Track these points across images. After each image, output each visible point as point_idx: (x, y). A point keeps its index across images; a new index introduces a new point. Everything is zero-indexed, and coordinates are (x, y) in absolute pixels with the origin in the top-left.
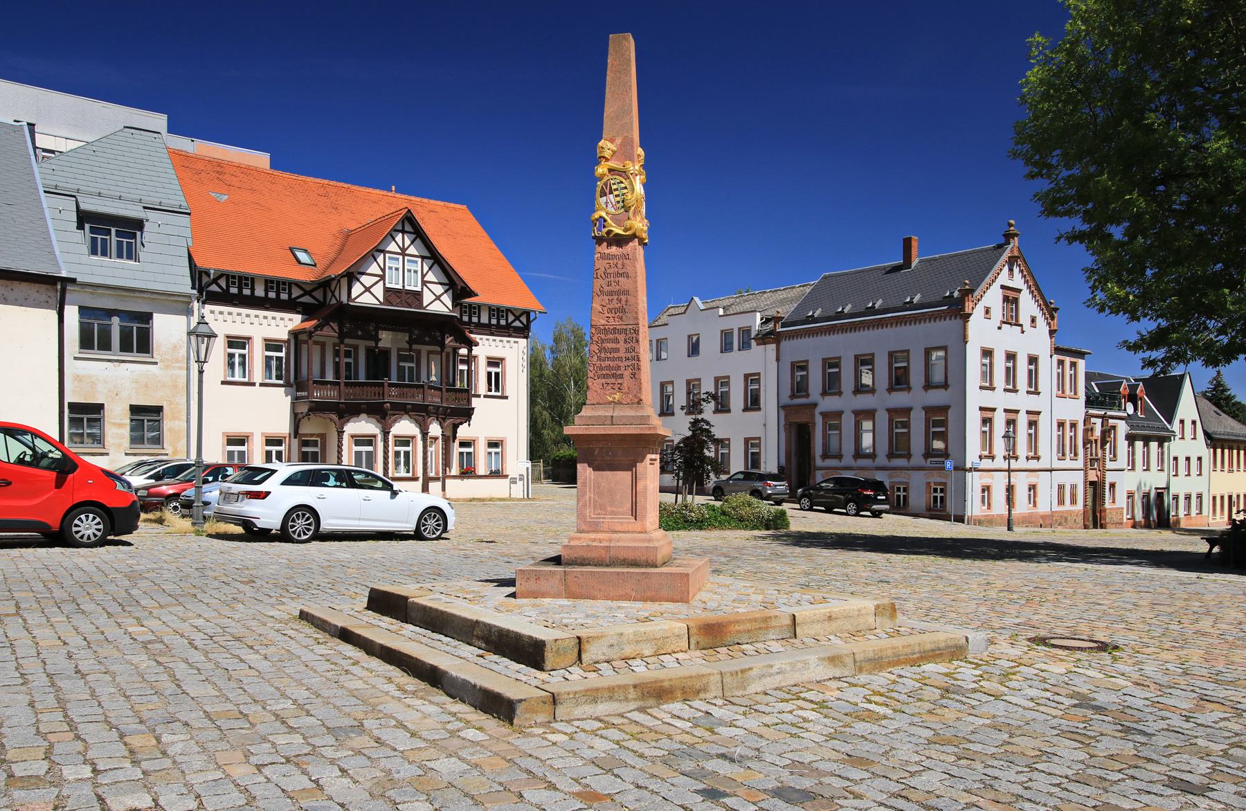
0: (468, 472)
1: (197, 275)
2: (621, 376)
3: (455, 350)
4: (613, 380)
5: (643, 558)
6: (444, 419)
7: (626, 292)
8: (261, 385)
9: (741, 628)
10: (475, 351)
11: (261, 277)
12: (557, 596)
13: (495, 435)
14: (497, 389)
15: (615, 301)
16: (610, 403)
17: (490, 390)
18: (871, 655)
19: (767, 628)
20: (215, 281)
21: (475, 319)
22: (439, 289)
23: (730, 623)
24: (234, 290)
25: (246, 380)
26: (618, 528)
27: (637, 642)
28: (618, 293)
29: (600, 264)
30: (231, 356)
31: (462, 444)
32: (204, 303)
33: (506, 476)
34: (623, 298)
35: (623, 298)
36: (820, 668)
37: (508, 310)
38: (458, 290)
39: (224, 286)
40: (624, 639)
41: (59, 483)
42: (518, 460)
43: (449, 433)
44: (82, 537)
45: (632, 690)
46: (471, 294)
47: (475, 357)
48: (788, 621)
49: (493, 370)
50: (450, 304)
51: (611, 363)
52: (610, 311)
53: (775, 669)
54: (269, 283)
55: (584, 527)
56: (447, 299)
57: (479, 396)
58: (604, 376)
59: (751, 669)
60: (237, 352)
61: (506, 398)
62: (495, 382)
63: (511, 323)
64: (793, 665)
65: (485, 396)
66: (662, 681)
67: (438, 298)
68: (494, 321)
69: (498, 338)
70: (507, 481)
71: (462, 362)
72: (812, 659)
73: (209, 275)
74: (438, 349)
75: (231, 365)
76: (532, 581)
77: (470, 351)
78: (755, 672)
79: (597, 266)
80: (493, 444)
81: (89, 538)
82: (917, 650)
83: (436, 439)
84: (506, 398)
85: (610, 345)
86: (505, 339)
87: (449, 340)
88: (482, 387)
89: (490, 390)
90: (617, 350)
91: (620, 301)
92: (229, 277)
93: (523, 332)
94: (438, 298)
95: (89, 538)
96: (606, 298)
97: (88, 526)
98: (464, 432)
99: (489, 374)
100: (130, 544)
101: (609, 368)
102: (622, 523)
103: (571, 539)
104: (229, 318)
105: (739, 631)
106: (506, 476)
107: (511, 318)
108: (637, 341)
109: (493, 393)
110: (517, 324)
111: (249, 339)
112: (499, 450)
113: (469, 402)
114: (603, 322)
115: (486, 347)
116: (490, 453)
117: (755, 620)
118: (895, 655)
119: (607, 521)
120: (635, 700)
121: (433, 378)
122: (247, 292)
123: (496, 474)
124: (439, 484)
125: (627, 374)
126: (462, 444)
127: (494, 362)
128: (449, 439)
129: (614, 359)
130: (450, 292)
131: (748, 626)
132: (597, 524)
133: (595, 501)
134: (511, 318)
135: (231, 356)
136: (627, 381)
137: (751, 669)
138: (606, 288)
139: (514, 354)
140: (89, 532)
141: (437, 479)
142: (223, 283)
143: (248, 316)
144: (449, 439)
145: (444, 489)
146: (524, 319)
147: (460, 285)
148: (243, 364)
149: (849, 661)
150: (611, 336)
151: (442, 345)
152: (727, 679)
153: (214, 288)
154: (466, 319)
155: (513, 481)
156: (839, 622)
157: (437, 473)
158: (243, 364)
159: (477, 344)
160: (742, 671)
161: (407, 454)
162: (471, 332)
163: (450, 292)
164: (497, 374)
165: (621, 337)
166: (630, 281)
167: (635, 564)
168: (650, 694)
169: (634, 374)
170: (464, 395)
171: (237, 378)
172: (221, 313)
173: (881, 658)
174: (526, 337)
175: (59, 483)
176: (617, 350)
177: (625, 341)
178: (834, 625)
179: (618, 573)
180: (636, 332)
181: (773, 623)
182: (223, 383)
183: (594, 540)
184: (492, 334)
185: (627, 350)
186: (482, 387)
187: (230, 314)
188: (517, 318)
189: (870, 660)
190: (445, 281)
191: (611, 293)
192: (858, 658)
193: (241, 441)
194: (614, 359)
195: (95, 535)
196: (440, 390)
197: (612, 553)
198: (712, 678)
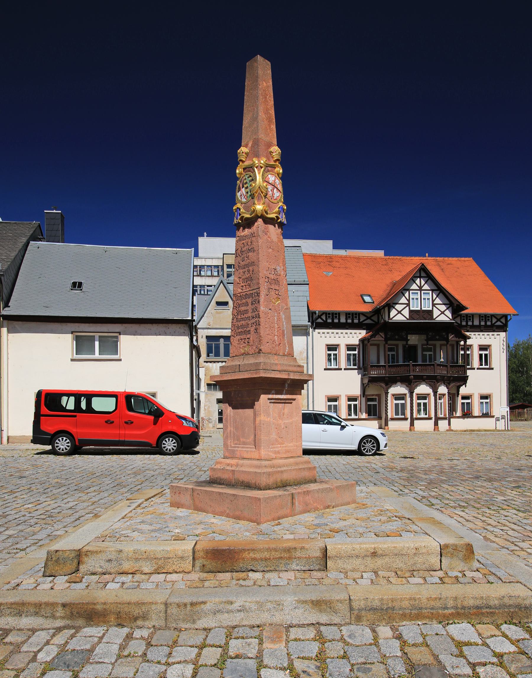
0: (467, 414)
1: (311, 315)
3: (458, 343)
5: (253, 481)
6: (449, 384)
7: (253, 264)
8: (345, 369)
9: (258, 556)
10: (469, 342)
11: (343, 312)
12: (188, 508)
13: (485, 392)
14: (486, 364)
15: (247, 272)
16: (243, 354)
17: (481, 365)
18: (376, 603)
19: (290, 558)
20: (319, 317)
21: (470, 323)
22: (443, 308)
23: (244, 550)
24: (329, 321)
25: (337, 367)
26: (245, 456)
27: (137, 560)
28: (247, 265)
30: (329, 355)
31: (464, 398)
32: (315, 329)
33: (493, 417)
34: (251, 268)
35: (251, 268)
36: (299, 612)
37: (493, 316)
38: (456, 307)
39: (324, 318)
40: (124, 555)
41: (155, 423)
42: (501, 406)
43: (454, 391)
44: (167, 450)
45: (60, 609)
46: (464, 308)
47: (471, 346)
48: (318, 554)
49: (483, 353)
50: (450, 316)
53: (236, 606)
54: (348, 315)
55: (227, 454)
56: (448, 313)
57: (474, 369)
59: (204, 603)
60: (332, 353)
61: (492, 369)
62: (485, 360)
63: (494, 323)
64: (260, 605)
65: (478, 369)
66: (95, 604)
67: (443, 313)
68: (483, 323)
69: (486, 333)
70: (494, 419)
71: (462, 349)
72: (289, 600)
73: (315, 313)
74: (445, 342)
75: (329, 360)
76: (177, 495)
77: (465, 342)
78: (208, 606)
80: (484, 397)
81: (170, 450)
82: (451, 603)
83: (444, 395)
84: (492, 369)
85: (243, 308)
86: (491, 333)
87: (451, 337)
88: (476, 362)
89: (481, 365)
90: (246, 311)
91: (249, 271)
92: (326, 313)
93: (503, 328)
94: (443, 313)
95: (170, 450)
96: (241, 271)
97: (169, 444)
98: (463, 390)
99: (481, 355)
100: (198, 453)
101: (242, 326)
102: (247, 452)
103: (217, 463)
104: (328, 335)
105: (254, 559)
106: (493, 417)
107: (494, 320)
108: (259, 302)
109: (484, 366)
110: (499, 323)
111: (338, 345)
112: (488, 401)
113: (465, 373)
114: (240, 290)
115: (476, 339)
116: (482, 403)
117: (276, 550)
118: (414, 607)
119: (241, 450)
120: (63, 618)
121: (442, 360)
122: (336, 321)
123: (486, 415)
124: (447, 421)
125: (252, 329)
126: (464, 398)
127: (483, 348)
128: (453, 396)
130: (450, 308)
131: (266, 555)
132: (233, 451)
133: (234, 434)
134: (494, 320)
135: (329, 355)
136: (252, 336)
137: (204, 603)
138: (242, 263)
139: (497, 342)
140: (169, 447)
141: (444, 419)
142: (324, 317)
143: (337, 333)
144: (453, 396)
145: (449, 424)
146: (503, 320)
147: (455, 303)
148: (335, 359)
149: (344, 608)
150: (244, 301)
151: (447, 340)
152: (173, 610)
153: (319, 320)
154: (464, 323)
155: (498, 419)
156: (387, 559)
157: (445, 415)
158: (335, 359)
159: (469, 338)
160: (192, 604)
161: (425, 404)
162: (468, 331)
163: (450, 308)
164: (486, 355)
165: (249, 301)
166: (255, 254)
167: (248, 486)
168: (80, 615)
169: (256, 329)
170: (462, 369)
171: (333, 367)
172: (323, 333)
173: (393, 609)
174: (505, 331)
175: (155, 423)
176: (246, 311)
177: (252, 304)
178: (379, 562)
179: (220, 493)
180: (258, 294)
181: (298, 554)
182: (325, 369)
183: (228, 465)
184: (482, 331)
185: (253, 311)
186: (476, 362)
187: (328, 333)
188: (499, 320)
189: (373, 610)
190: (448, 302)
192: (355, 605)
193: (334, 399)
195: (173, 449)
196: (446, 366)
197: (237, 476)
198: (154, 607)
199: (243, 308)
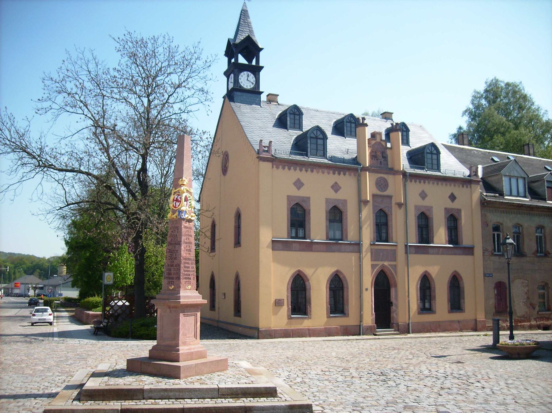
2: (190, 279)
4: (188, 280)
29: (184, 230)
51: (188, 273)
52: (187, 250)
58: (186, 278)
79: (183, 231)
85: (187, 265)
90: (189, 267)
101: (187, 275)
129: (188, 271)
138: (186, 241)
165: (190, 262)
183: (188, 349)
191: (186, 243)
194: (188, 271)
199: (187, 265)
